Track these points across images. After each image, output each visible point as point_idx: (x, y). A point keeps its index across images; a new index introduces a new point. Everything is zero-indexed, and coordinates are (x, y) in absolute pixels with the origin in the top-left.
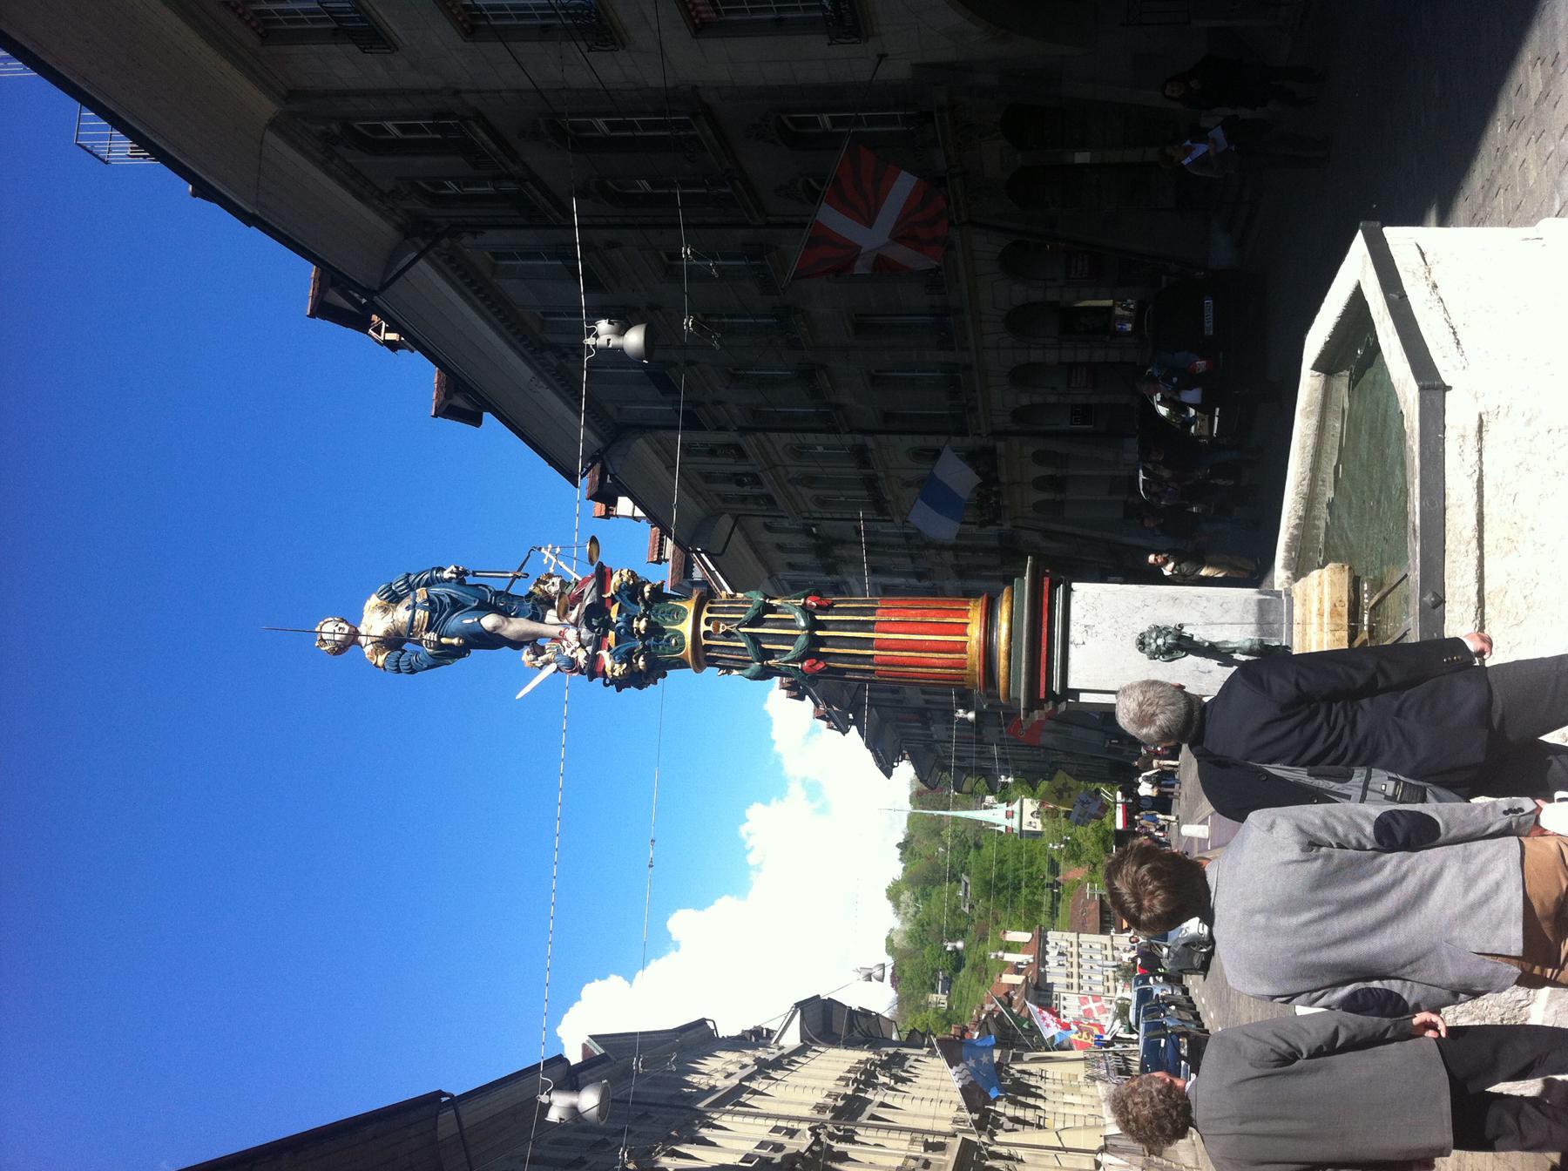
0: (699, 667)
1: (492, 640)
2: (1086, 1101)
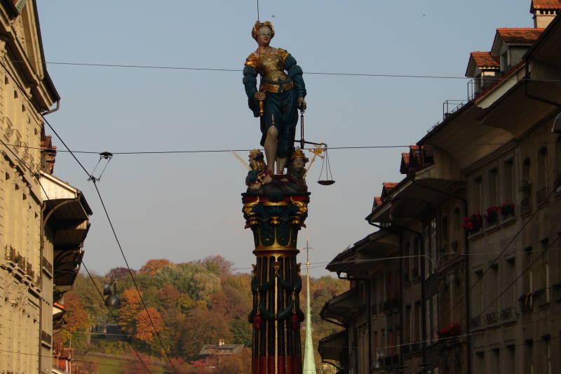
0: (254, 252)
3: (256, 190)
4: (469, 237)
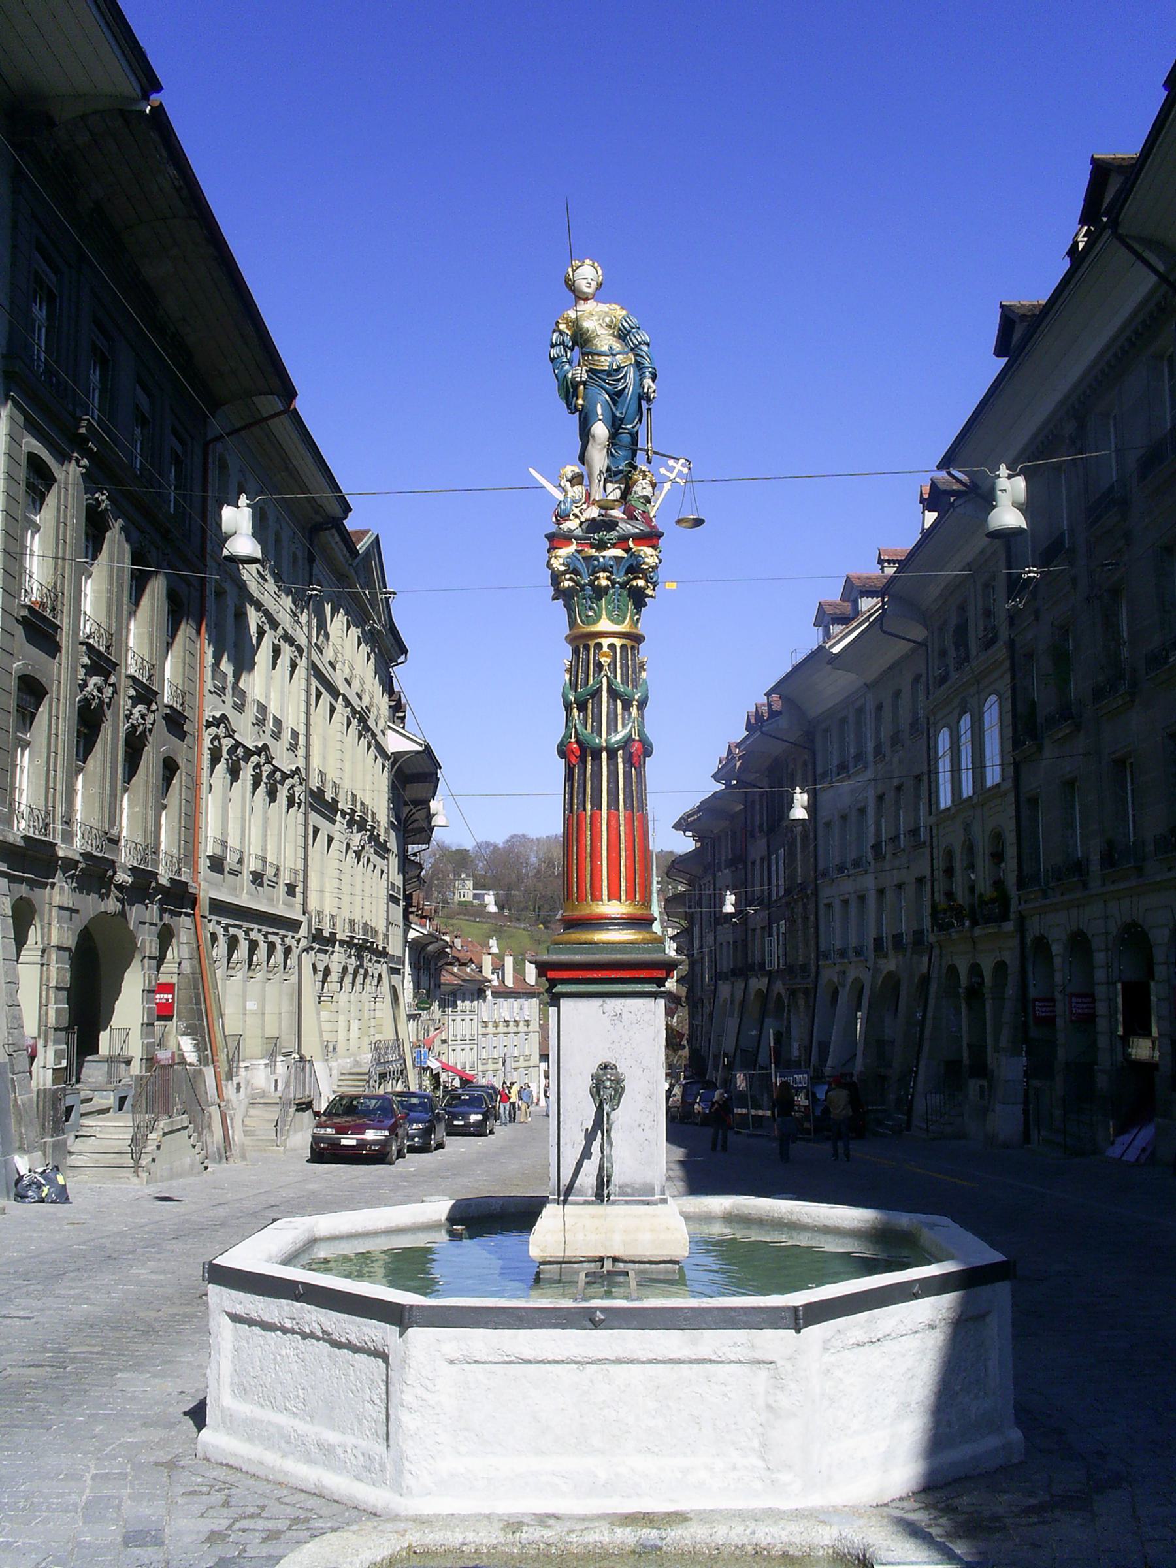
0: (571, 639)
1: (585, 434)
2: (354, 1043)
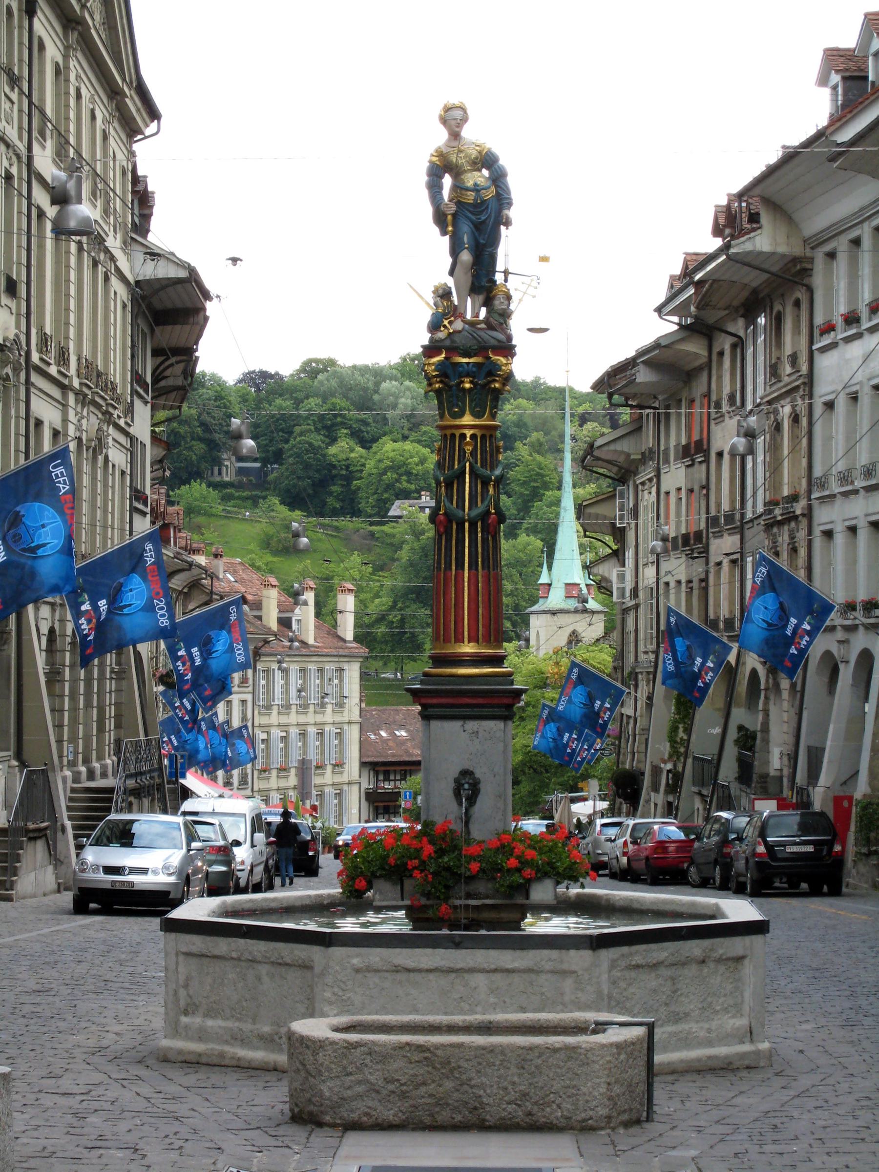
3: (442, 340)
4: (814, 348)
